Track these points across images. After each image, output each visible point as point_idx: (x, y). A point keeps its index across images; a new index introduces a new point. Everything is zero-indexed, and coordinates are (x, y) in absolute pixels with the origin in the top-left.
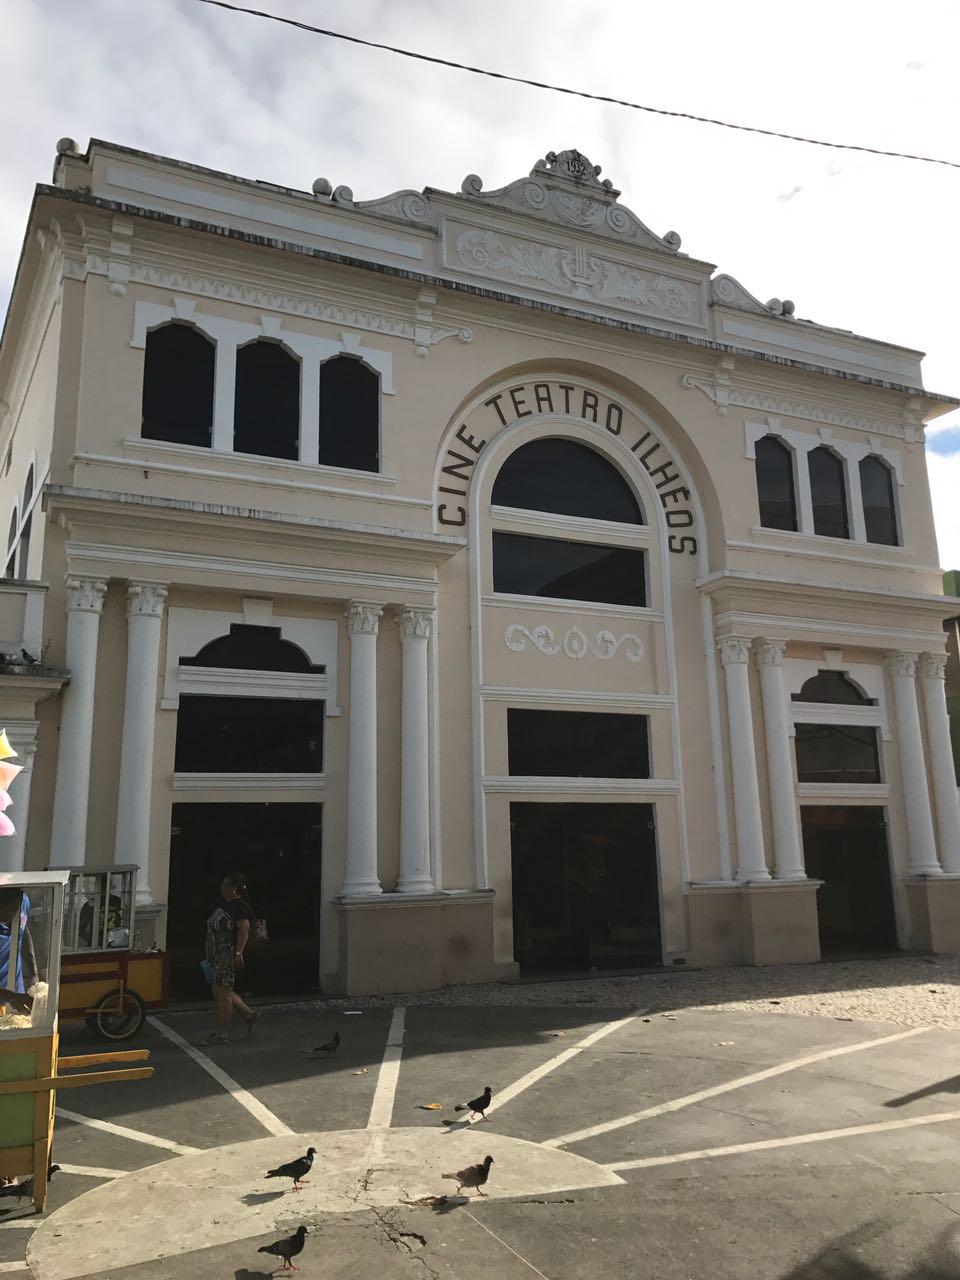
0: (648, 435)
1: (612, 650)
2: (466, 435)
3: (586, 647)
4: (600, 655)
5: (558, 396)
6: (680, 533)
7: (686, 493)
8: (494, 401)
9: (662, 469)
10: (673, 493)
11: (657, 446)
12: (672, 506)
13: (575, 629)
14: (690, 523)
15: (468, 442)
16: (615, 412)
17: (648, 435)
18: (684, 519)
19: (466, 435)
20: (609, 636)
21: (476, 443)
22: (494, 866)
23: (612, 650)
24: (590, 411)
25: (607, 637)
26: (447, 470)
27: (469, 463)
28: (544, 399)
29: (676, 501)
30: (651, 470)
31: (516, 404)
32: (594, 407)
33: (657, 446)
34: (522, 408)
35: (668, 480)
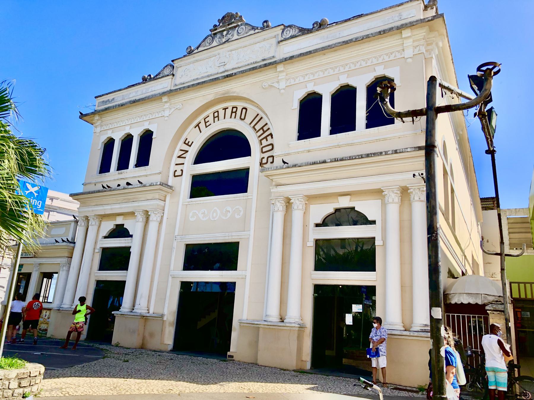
0: (258, 115)
1: (229, 215)
2: (187, 142)
3: (219, 215)
4: (224, 218)
5: (222, 113)
6: (266, 155)
7: (271, 135)
8: (198, 125)
9: (262, 128)
10: (266, 138)
11: (262, 118)
12: (264, 143)
13: (216, 208)
14: (272, 149)
15: (187, 144)
16: (244, 110)
17: (258, 115)
18: (270, 147)
19: (187, 142)
20: (229, 209)
21: (190, 144)
22: (169, 307)
23: (229, 215)
24: (234, 114)
25: (228, 210)
26: (179, 157)
27: (187, 151)
28: (216, 116)
29: (267, 140)
30: (257, 130)
31: (206, 123)
32: (236, 112)
33: (262, 118)
34: (207, 124)
35: (264, 132)
